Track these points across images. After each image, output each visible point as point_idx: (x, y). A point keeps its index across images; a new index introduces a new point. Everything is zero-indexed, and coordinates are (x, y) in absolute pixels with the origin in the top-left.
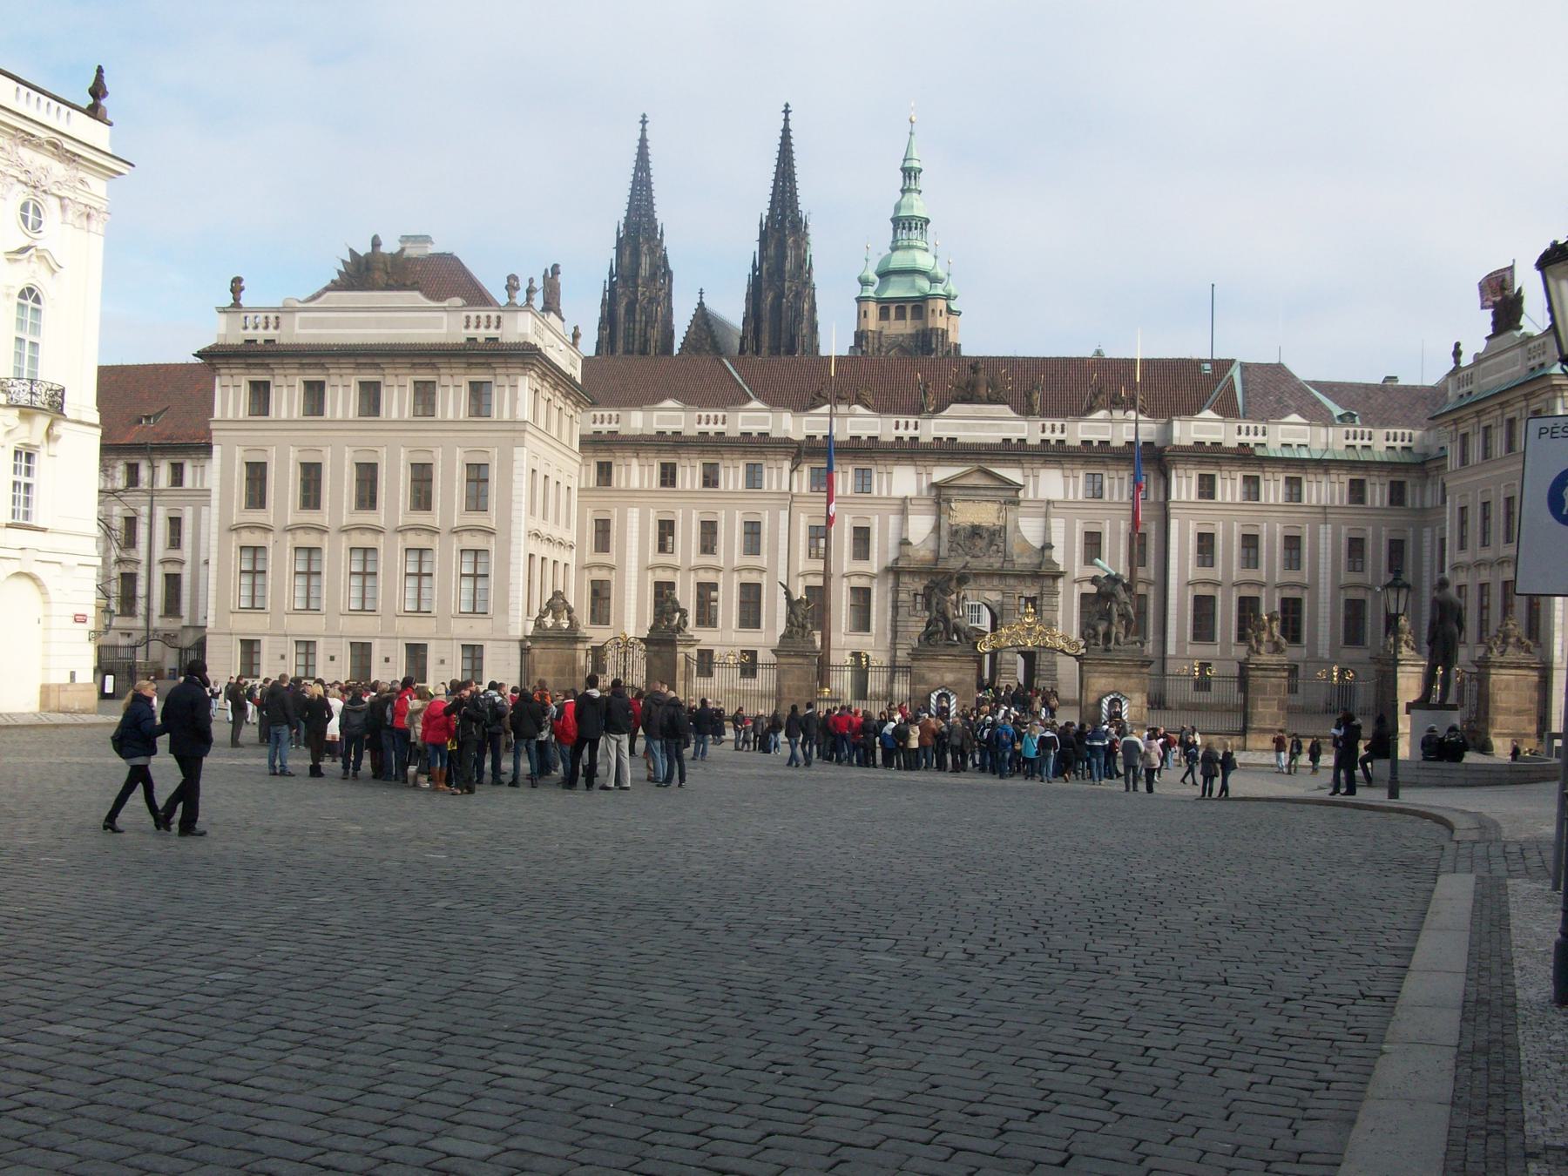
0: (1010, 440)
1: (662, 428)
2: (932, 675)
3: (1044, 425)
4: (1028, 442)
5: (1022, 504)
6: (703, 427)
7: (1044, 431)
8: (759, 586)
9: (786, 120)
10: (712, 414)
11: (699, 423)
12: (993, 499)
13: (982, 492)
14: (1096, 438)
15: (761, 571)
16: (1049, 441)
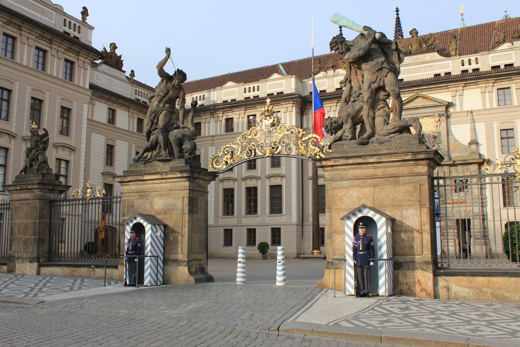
0: (439, 74)
1: (225, 99)
2: (141, 202)
3: (463, 61)
4: (452, 74)
5: (452, 116)
6: (247, 95)
7: (463, 65)
8: (280, 186)
9: (398, 14)
10: (252, 86)
11: (245, 92)
12: (431, 114)
13: (422, 111)
14: (502, 63)
15: (282, 176)
16: (467, 71)
